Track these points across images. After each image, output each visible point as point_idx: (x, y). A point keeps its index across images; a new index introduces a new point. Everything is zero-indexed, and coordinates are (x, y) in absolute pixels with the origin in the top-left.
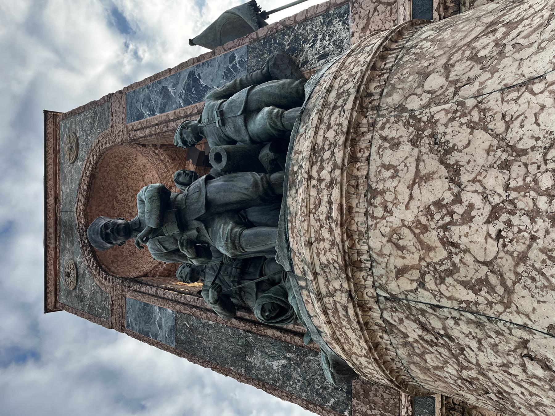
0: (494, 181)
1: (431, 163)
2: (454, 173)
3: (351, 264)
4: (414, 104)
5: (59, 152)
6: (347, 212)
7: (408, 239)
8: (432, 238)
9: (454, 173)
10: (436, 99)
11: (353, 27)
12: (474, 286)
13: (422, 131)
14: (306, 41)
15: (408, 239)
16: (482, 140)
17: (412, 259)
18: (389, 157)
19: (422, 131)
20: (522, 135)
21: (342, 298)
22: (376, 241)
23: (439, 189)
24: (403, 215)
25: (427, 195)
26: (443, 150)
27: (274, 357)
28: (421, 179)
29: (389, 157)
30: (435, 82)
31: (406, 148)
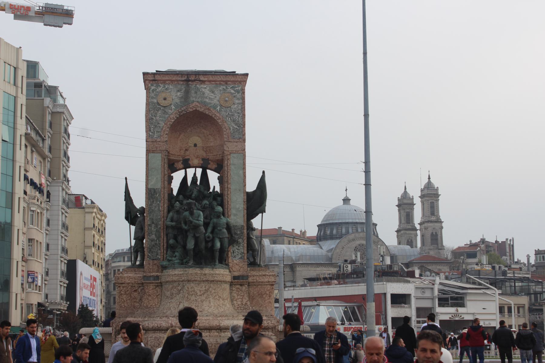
0: (199, 300)
1: (202, 292)
2: (201, 295)
3: (189, 281)
4: (211, 289)
5: (226, 84)
6: (196, 281)
7: (193, 289)
8: (193, 293)
9: (201, 295)
10: (211, 292)
11: (238, 261)
12: (187, 297)
13: (207, 291)
14: (239, 247)
15: (193, 289)
16: (204, 298)
17: (190, 290)
18: (204, 286)
19: (207, 291)
20: (204, 303)
21: (183, 279)
22: (192, 285)
23: (199, 293)
24: (196, 289)
25: (198, 292)
26: (203, 294)
27: (156, 235)
28: (200, 291)
29: (204, 286)
30: (213, 291)
31: (204, 289)
